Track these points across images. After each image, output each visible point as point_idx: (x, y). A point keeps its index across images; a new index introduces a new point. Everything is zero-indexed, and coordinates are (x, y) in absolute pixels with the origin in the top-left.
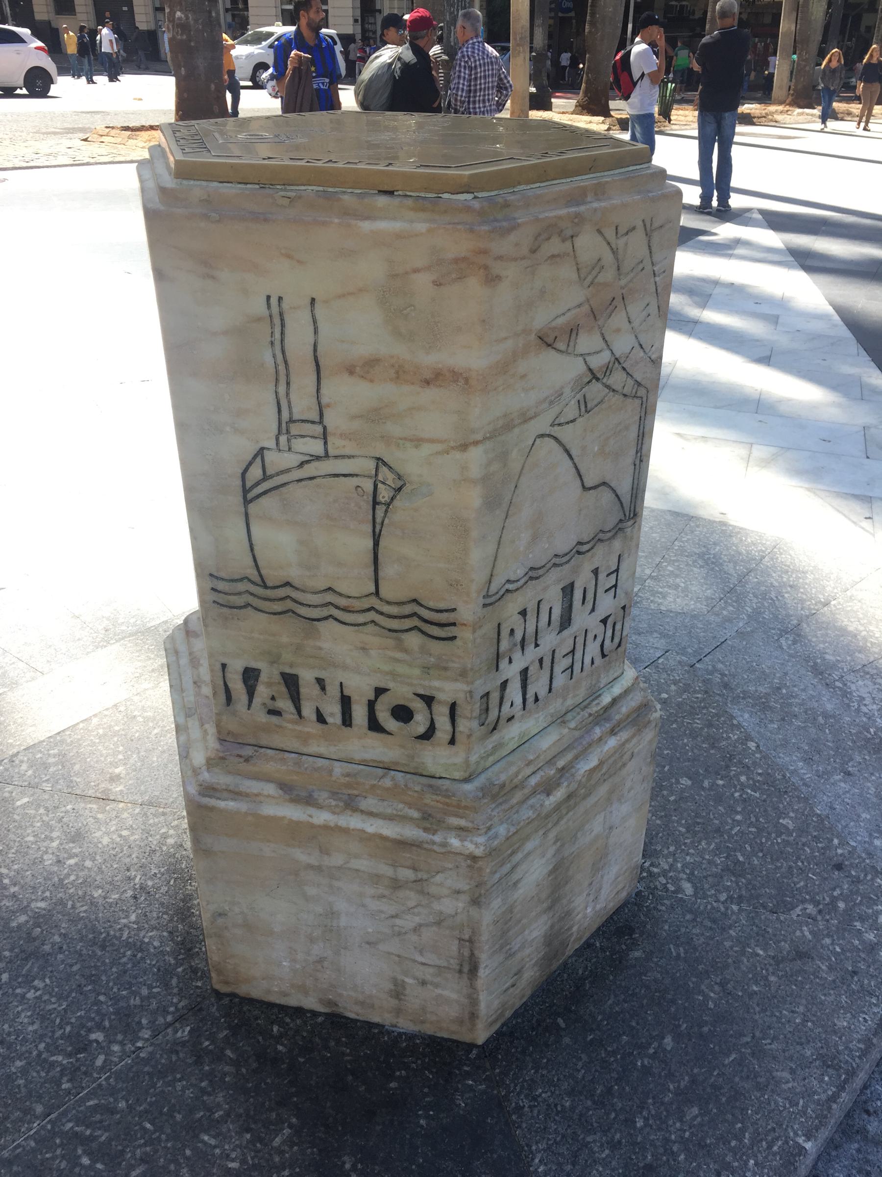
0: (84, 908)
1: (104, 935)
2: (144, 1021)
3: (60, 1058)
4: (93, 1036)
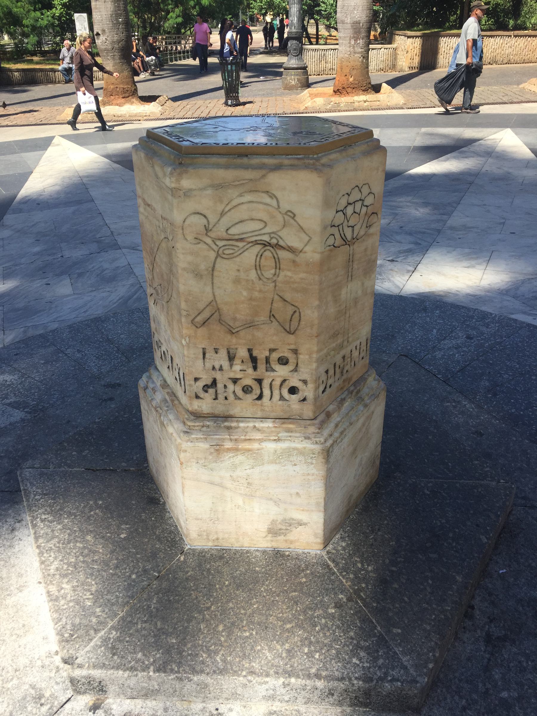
0: (402, 541)
1: (402, 524)
2: (408, 485)
3: (443, 494)
4: (428, 493)
